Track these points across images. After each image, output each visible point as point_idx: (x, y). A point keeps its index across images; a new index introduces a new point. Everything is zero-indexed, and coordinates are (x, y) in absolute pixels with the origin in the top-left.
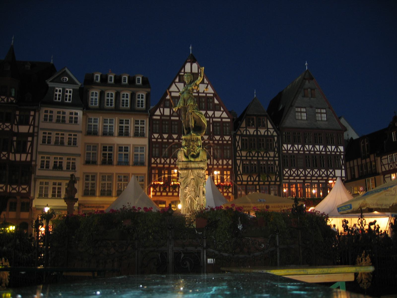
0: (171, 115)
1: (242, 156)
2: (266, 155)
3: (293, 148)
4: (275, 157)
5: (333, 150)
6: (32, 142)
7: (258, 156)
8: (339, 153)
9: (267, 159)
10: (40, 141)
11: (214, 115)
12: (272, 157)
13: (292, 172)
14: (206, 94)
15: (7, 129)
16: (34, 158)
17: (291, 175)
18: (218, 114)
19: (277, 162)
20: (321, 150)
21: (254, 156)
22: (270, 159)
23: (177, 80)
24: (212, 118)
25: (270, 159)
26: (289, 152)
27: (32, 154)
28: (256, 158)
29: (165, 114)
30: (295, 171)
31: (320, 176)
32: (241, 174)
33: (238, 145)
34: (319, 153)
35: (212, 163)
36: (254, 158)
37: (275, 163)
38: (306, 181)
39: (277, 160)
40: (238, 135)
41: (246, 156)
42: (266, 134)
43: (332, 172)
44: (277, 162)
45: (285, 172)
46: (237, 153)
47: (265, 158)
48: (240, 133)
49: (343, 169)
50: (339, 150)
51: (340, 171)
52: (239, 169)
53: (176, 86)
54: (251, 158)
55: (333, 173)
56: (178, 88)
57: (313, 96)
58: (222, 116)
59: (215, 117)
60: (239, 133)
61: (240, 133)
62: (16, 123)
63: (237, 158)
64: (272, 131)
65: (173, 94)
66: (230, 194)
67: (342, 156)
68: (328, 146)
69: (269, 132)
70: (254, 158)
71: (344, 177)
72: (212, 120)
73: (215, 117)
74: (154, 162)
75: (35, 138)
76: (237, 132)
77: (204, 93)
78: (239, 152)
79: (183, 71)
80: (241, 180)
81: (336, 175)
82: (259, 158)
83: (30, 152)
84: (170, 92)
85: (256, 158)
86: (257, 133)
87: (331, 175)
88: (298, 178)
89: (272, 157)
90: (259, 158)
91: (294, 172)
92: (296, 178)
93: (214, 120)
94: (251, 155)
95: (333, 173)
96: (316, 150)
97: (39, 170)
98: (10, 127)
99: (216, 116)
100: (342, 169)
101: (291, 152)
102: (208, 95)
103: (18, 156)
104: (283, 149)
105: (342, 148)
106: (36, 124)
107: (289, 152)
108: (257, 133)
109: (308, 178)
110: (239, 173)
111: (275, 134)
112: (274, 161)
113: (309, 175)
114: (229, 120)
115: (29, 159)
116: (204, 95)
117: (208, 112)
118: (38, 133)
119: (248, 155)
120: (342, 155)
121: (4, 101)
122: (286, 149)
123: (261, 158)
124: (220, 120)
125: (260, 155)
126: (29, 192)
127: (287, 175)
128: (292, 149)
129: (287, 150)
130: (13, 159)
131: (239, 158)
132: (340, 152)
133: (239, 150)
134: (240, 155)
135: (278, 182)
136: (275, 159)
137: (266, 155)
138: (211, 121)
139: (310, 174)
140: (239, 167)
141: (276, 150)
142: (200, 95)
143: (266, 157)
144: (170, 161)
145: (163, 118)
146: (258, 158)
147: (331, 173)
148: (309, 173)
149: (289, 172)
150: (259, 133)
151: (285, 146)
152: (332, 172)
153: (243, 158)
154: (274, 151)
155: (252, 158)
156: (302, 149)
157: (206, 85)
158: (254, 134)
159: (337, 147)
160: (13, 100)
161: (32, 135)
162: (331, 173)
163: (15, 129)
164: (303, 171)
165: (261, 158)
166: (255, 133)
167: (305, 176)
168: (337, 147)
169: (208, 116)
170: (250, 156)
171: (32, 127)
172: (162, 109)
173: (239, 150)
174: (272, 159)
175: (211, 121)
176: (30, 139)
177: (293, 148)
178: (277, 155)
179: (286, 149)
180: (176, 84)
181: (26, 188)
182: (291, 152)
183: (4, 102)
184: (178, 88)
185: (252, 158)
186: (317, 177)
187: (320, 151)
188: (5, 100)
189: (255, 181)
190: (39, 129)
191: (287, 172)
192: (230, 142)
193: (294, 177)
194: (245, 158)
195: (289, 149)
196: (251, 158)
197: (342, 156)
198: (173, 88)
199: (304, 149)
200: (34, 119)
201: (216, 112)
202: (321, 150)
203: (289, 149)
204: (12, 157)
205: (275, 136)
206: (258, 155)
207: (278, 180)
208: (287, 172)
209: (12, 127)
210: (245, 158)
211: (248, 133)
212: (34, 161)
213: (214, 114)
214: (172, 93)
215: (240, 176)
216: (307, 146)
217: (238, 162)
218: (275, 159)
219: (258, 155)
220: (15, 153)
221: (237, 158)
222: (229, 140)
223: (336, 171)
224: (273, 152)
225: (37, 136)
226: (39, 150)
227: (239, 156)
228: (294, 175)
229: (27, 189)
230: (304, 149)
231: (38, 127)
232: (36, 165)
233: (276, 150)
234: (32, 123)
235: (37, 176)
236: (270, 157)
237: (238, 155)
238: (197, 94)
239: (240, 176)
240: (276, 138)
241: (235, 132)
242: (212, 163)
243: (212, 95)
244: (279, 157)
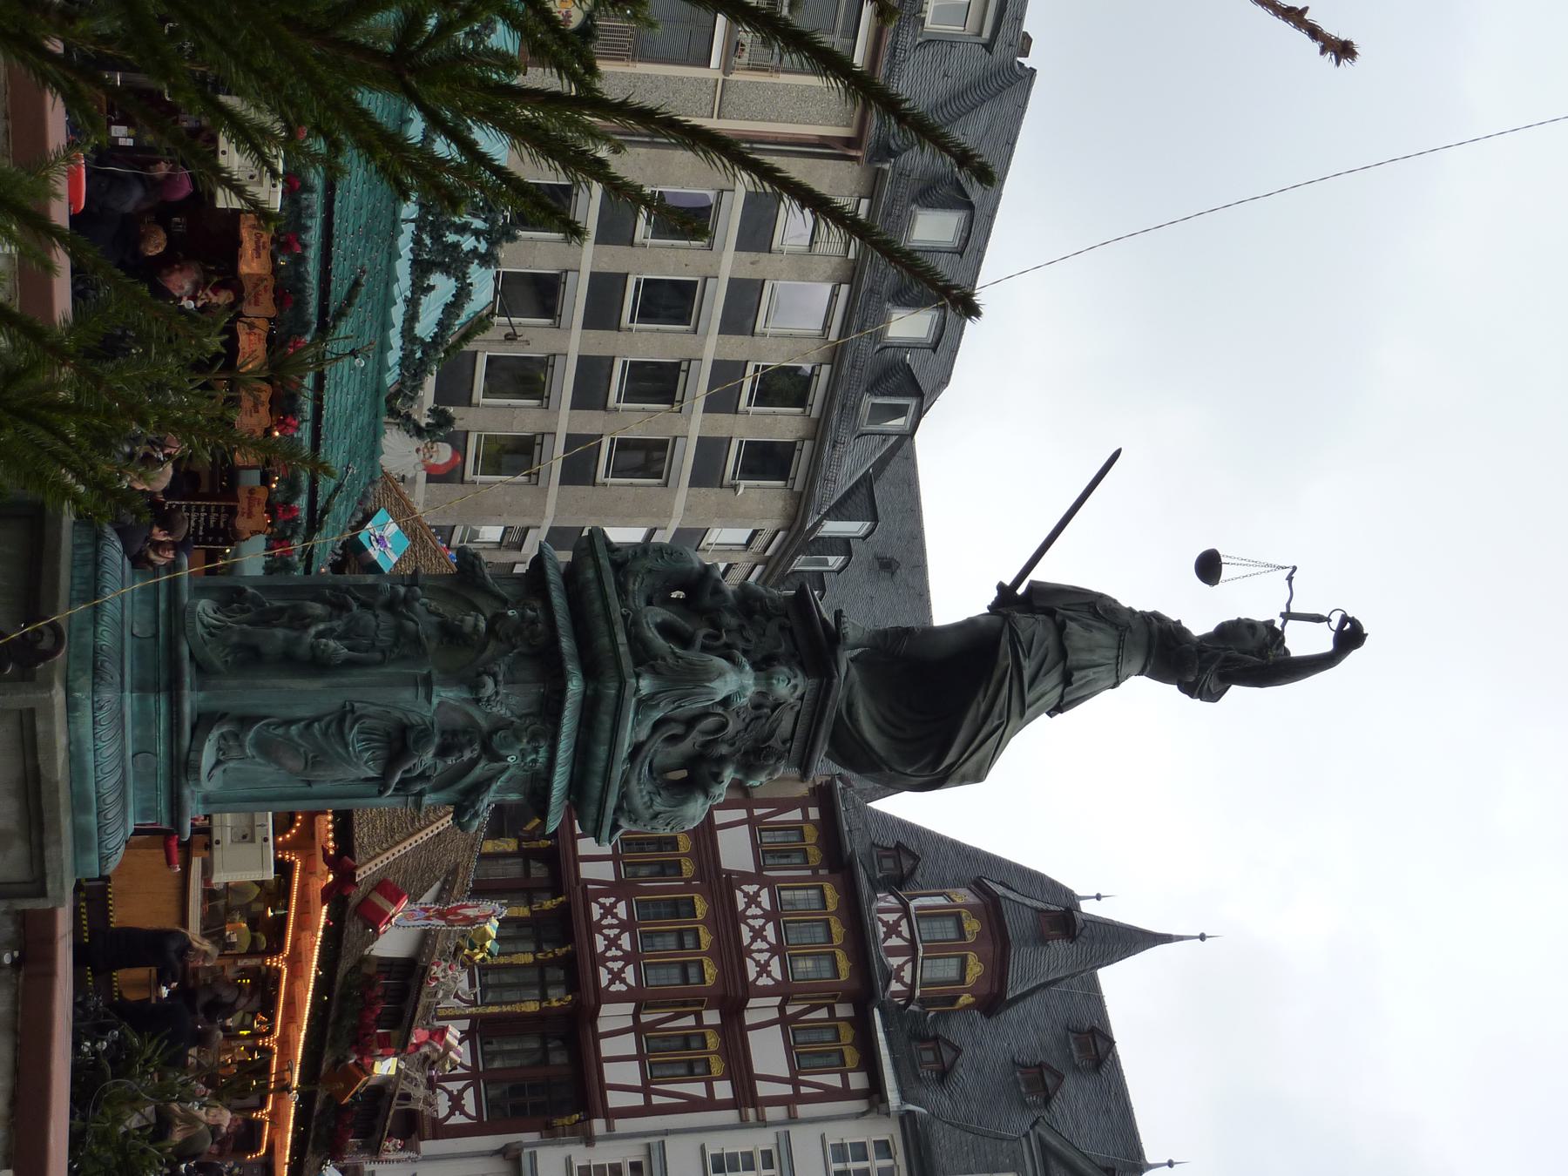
6: (710, 1104)
10: (720, 1144)
15: (752, 971)
16: (621, 1125)
27: (648, 1110)
62: (790, 1010)
75: (731, 1116)
83: (656, 1100)
97: (568, 1162)
98: (764, 981)
103: (627, 1045)
106: (803, 1110)
115: (615, 1100)
118: (762, 1123)
121: (888, 936)
126: (441, 1130)
130: (603, 1026)
160: (900, 980)
161: (745, 1097)
163: (759, 1010)
171: (787, 1090)
176: (723, 1090)
181: (463, 1113)
183: (882, 936)
188: (894, 941)
190: (781, 1129)
200: (829, 1094)
204: (613, 1016)
209: (765, 992)
212: (610, 1127)
220: (638, 1028)
225: (743, 1124)
226: (670, 1142)
229: (458, 1119)
231: (793, 1119)
232: (589, 1140)
234: (804, 1090)
235: (533, 1156)
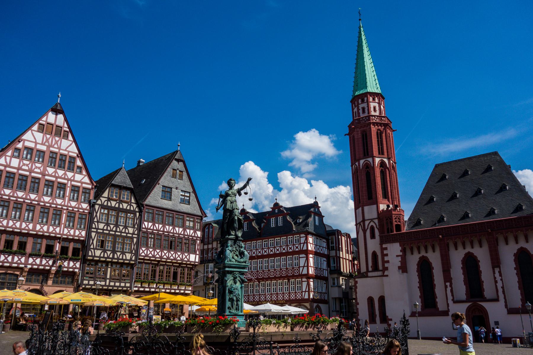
0: (19, 169)
1: (98, 229)
2: (125, 230)
3: (153, 227)
4: (133, 234)
5: (191, 235)
7: (116, 231)
8: (195, 238)
9: (125, 235)
11: (74, 178)
12: (130, 234)
13: (149, 252)
14: (69, 152)
17: (147, 255)
18: (78, 177)
19: (135, 240)
20: (180, 233)
21: (112, 231)
22: (128, 235)
23: (35, 127)
24: (71, 181)
25: (128, 235)
26: (149, 231)
28: (113, 233)
29: (11, 165)
30: (152, 251)
31: (175, 259)
32: (94, 249)
33: (96, 216)
34: (178, 235)
35: (61, 232)
36: (111, 232)
37: (133, 241)
38: (161, 263)
39: (135, 237)
40: (98, 204)
41: (103, 230)
42: (128, 208)
43: (187, 255)
44: (135, 240)
45: (141, 251)
46: (93, 224)
47: (123, 234)
48: (101, 203)
49: (198, 254)
50: (196, 235)
51: (194, 255)
52: (93, 243)
53: (33, 134)
54: (108, 232)
55: (188, 257)
56: (35, 139)
57: (181, 178)
58: (83, 181)
59: (74, 181)
60: (99, 202)
61: (101, 203)
63: (93, 230)
64: (135, 206)
65: (27, 144)
66: (77, 270)
67: (198, 241)
68: (187, 230)
69: (132, 207)
70: (111, 232)
71: (197, 262)
72: (71, 183)
73: (74, 181)
74: (53, 231)
76: (97, 202)
77: (66, 150)
78: (96, 223)
79: (44, 119)
80: (93, 255)
81: (191, 260)
82: (117, 233)
84: (25, 140)
85: (113, 233)
86: (119, 205)
87: (186, 259)
88: (154, 259)
89: (130, 234)
90: (117, 233)
91: (151, 252)
92: (152, 258)
93: (73, 183)
94: (109, 229)
95: (188, 257)
96: (175, 232)
99: (76, 179)
100: (196, 254)
101: (151, 231)
102: (71, 154)
104: (144, 226)
105: (199, 234)
107: (149, 231)
108: (119, 205)
109: (163, 260)
110: (92, 247)
111: (137, 210)
112: (132, 238)
113: (165, 257)
114: (90, 187)
116: (66, 153)
117: (67, 173)
119: (105, 228)
120: (198, 240)
122: (147, 227)
123: (119, 234)
124: (79, 184)
125: (118, 230)
127: (143, 254)
128: (152, 228)
129: (147, 229)
131: (95, 230)
132: (197, 237)
133: (96, 222)
134: (97, 227)
135: (133, 261)
136: (134, 236)
137: (125, 230)
138: (69, 185)
139: (166, 256)
140: (93, 240)
141: (136, 227)
142: (61, 151)
143: (125, 233)
144: (8, 223)
145: (8, 169)
146: (115, 233)
147: (186, 257)
148: (165, 254)
149: (145, 252)
150: (121, 207)
151: (146, 223)
152: (187, 255)
153: (99, 231)
154: (134, 227)
155: (109, 232)
156: (162, 230)
157: (71, 142)
158: (127, 208)
159: (195, 232)
162: (186, 257)
164: (159, 252)
165: (119, 234)
166: (117, 206)
167: (161, 257)
168: (195, 232)
169: (66, 177)
170: (107, 230)
172: (8, 159)
173: (96, 222)
174: (131, 235)
175: (69, 185)
177: (153, 227)
178: (136, 233)
179: (147, 227)
180: (33, 132)
182: (151, 231)
184: (35, 139)
185: (109, 232)
186: (172, 260)
187: (179, 234)
189: (108, 257)
191: (143, 252)
192: (87, 211)
193: (150, 257)
194: (101, 231)
195: (149, 227)
196: (108, 232)
197: (198, 241)
198: (28, 136)
199: (164, 229)
201: (76, 175)
202: (180, 233)
203: (149, 228)
205: (137, 212)
206: (116, 229)
207: (133, 259)
208: (143, 252)
210: (101, 231)
211: (109, 204)
213: (74, 176)
214: (26, 142)
215: (93, 250)
216: (167, 227)
217: (93, 234)
218: (134, 236)
219: (116, 229)
221: (93, 230)
222: (86, 209)
223: (191, 255)
224: (133, 229)
227: (95, 228)
228: (150, 255)
230: (164, 229)
233: (136, 227)
236: (129, 233)
237: (94, 226)
238: (57, 150)
239: (93, 250)
240: (138, 214)
241: (95, 201)
242: (61, 232)
243: (75, 155)
244: (138, 235)
